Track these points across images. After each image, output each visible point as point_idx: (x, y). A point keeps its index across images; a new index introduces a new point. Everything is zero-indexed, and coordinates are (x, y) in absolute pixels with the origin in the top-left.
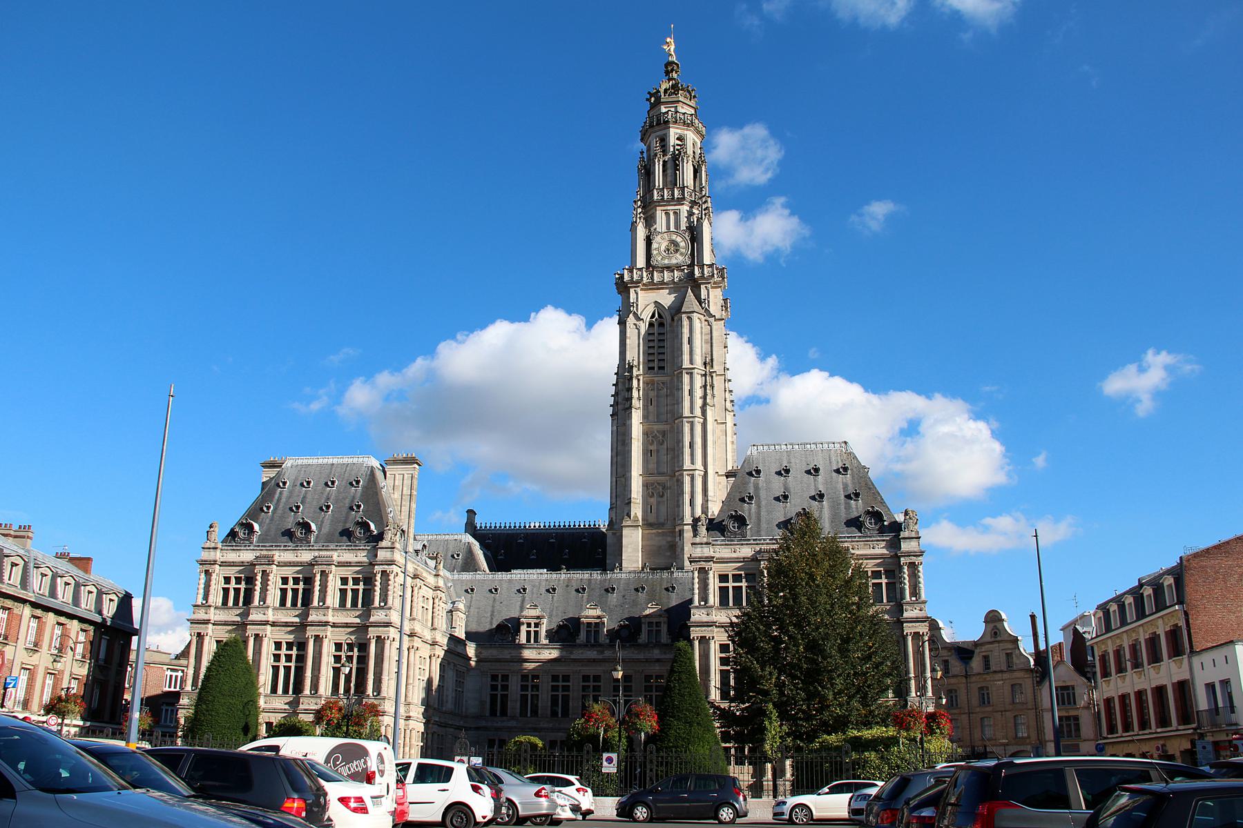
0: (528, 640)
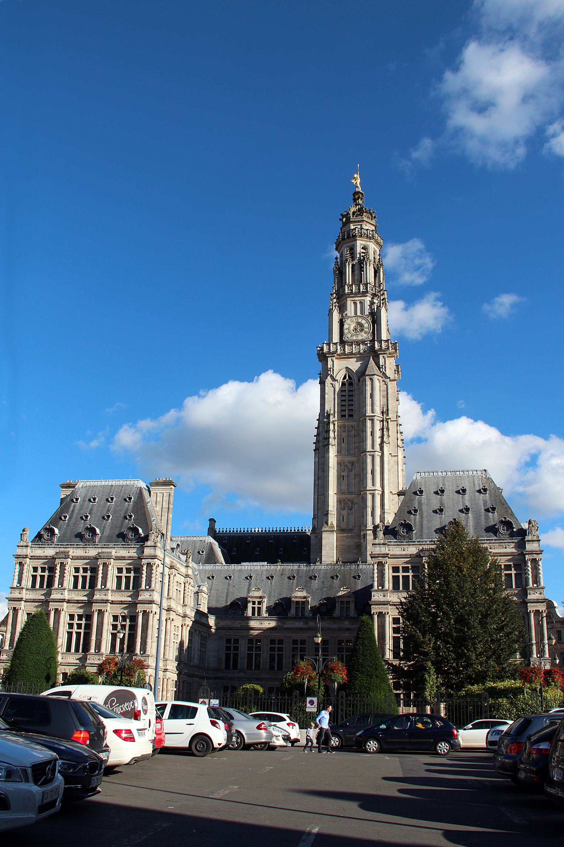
0: (253, 614)
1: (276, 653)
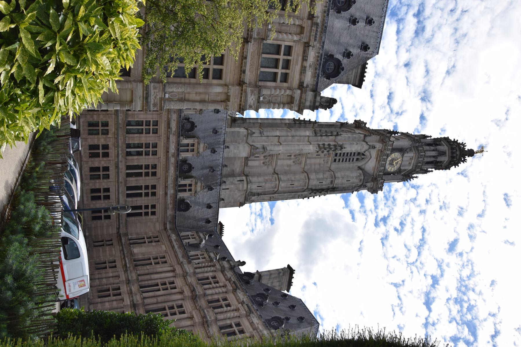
1: (144, 127)
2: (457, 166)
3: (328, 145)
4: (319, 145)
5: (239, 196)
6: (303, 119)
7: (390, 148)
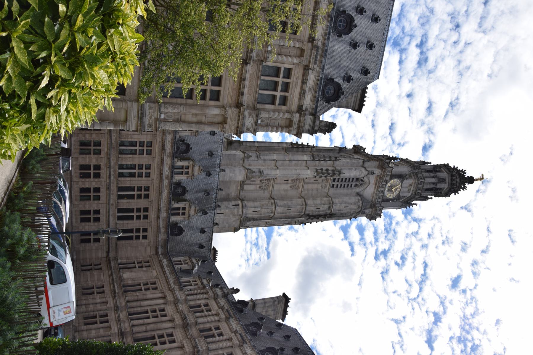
1: (138, 148)
2: (457, 194)
3: (326, 170)
4: (317, 170)
5: (234, 221)
6: (301, 143)
7: (390, 174)
